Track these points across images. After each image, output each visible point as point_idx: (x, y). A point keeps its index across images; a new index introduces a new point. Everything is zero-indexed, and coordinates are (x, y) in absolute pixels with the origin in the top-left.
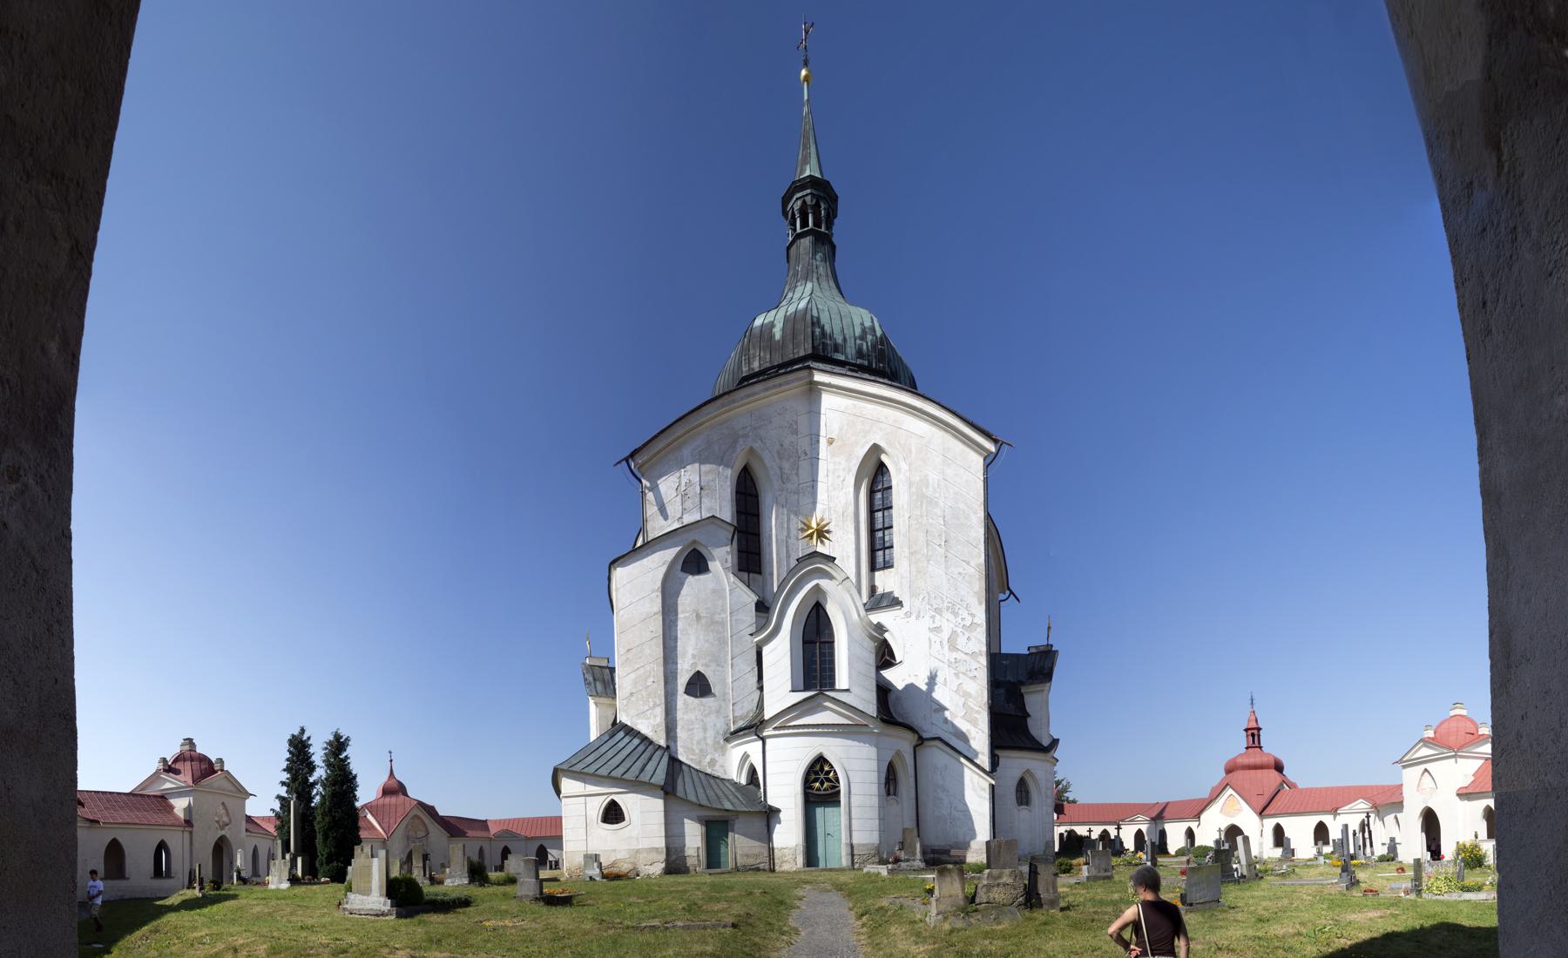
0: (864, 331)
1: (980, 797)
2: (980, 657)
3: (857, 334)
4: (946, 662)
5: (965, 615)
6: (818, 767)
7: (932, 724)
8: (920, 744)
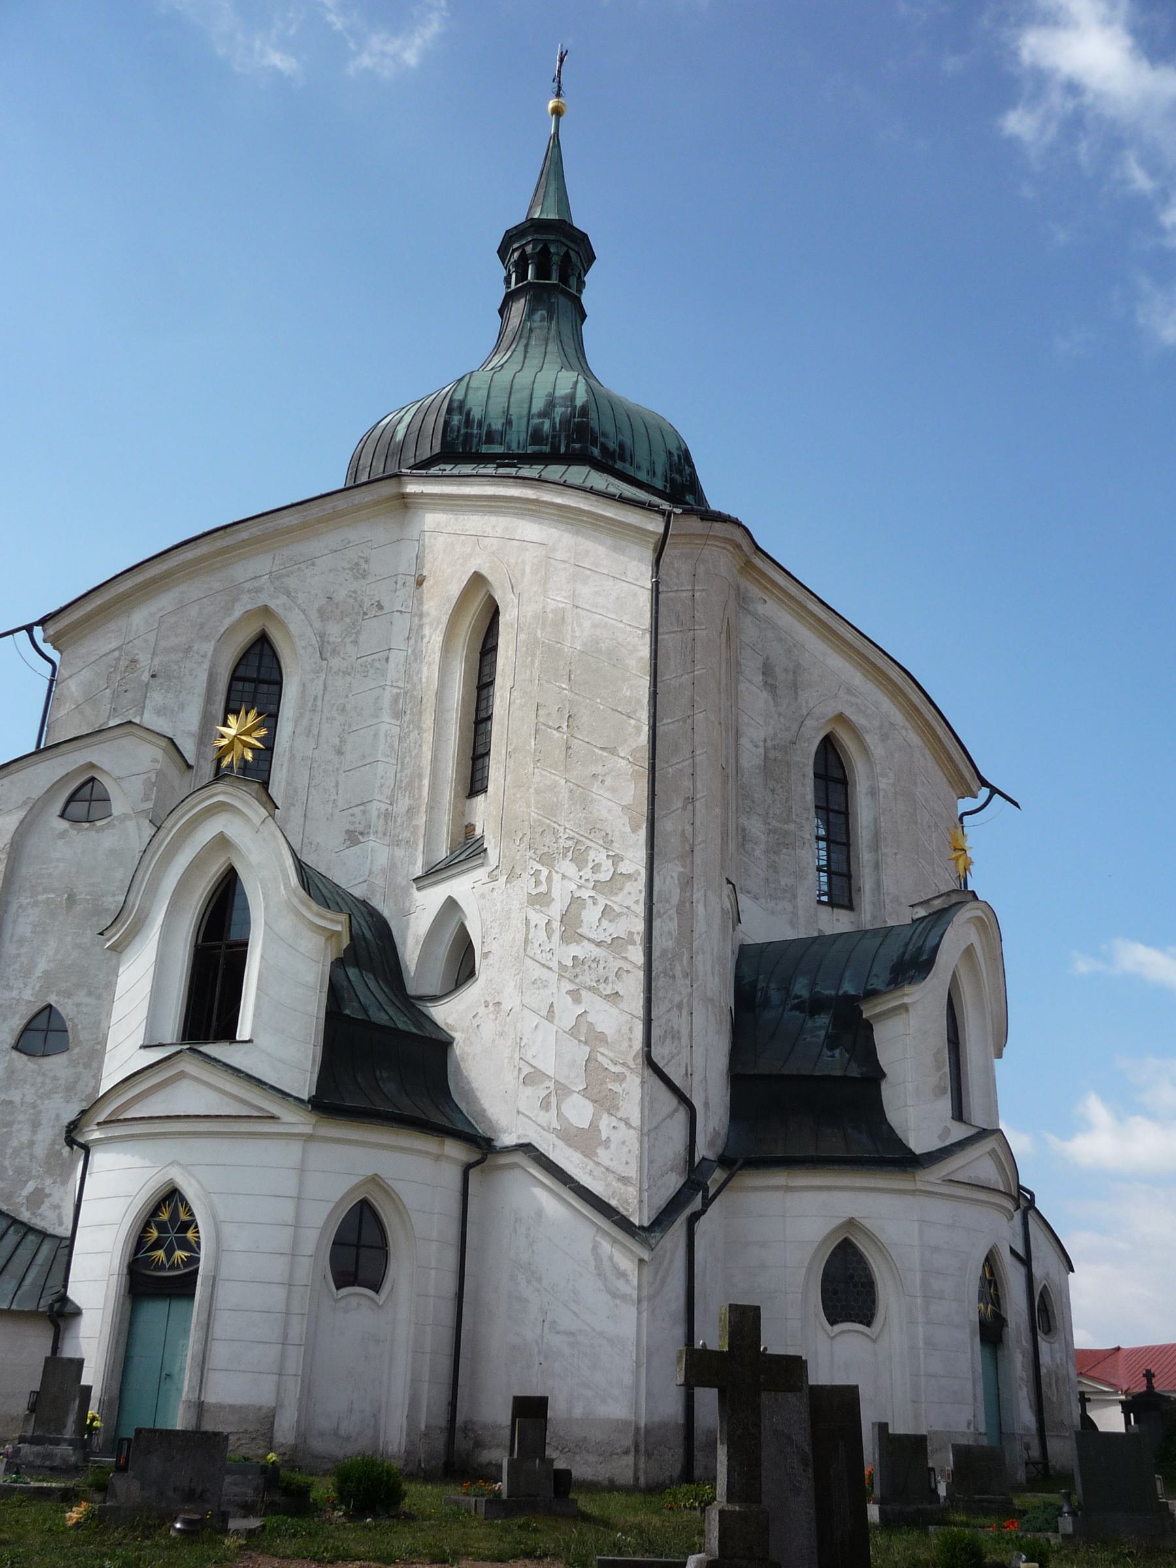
0: (551, 404)
1: (614, 1295)
2: (630, 947)
3: (535, 410)
4: (555, 967)
5: (601, 856)
6: (165, 1216)
7: (518, 1112)
8: (478, 1163)
